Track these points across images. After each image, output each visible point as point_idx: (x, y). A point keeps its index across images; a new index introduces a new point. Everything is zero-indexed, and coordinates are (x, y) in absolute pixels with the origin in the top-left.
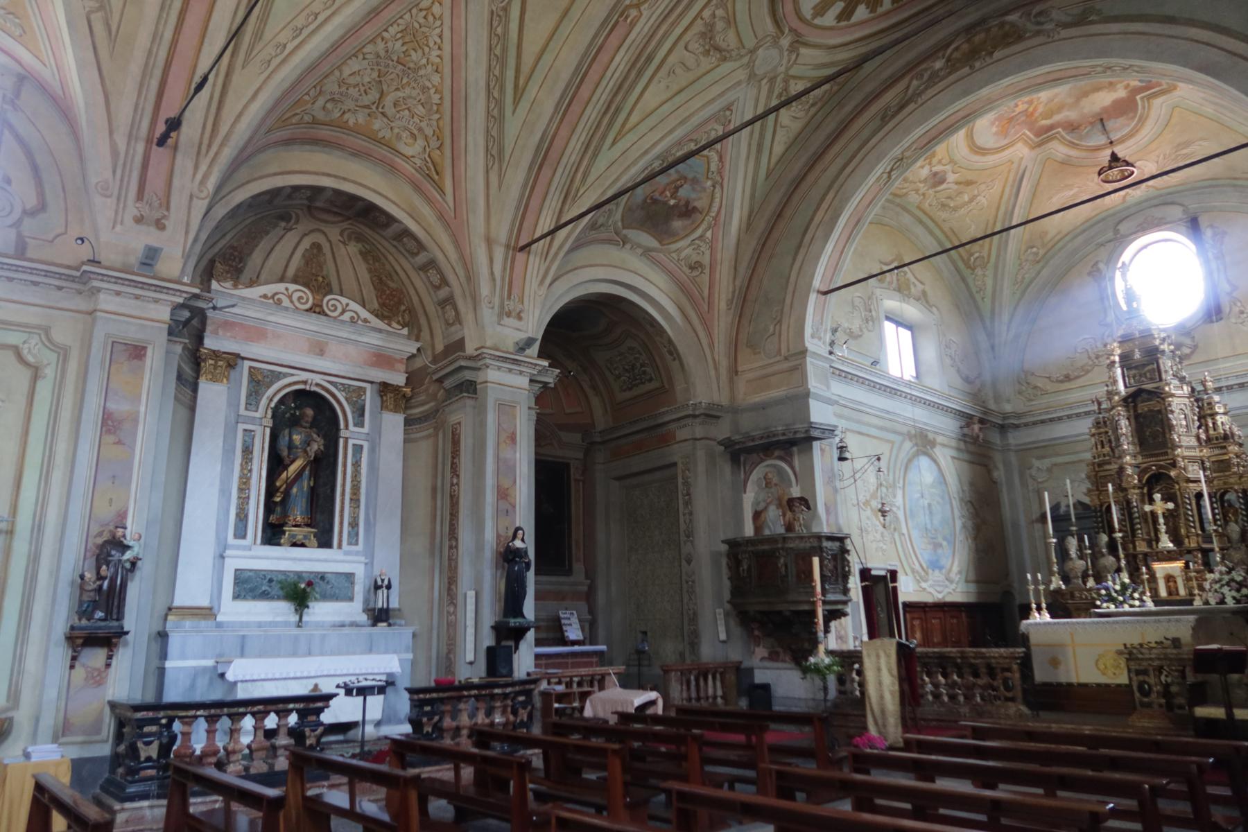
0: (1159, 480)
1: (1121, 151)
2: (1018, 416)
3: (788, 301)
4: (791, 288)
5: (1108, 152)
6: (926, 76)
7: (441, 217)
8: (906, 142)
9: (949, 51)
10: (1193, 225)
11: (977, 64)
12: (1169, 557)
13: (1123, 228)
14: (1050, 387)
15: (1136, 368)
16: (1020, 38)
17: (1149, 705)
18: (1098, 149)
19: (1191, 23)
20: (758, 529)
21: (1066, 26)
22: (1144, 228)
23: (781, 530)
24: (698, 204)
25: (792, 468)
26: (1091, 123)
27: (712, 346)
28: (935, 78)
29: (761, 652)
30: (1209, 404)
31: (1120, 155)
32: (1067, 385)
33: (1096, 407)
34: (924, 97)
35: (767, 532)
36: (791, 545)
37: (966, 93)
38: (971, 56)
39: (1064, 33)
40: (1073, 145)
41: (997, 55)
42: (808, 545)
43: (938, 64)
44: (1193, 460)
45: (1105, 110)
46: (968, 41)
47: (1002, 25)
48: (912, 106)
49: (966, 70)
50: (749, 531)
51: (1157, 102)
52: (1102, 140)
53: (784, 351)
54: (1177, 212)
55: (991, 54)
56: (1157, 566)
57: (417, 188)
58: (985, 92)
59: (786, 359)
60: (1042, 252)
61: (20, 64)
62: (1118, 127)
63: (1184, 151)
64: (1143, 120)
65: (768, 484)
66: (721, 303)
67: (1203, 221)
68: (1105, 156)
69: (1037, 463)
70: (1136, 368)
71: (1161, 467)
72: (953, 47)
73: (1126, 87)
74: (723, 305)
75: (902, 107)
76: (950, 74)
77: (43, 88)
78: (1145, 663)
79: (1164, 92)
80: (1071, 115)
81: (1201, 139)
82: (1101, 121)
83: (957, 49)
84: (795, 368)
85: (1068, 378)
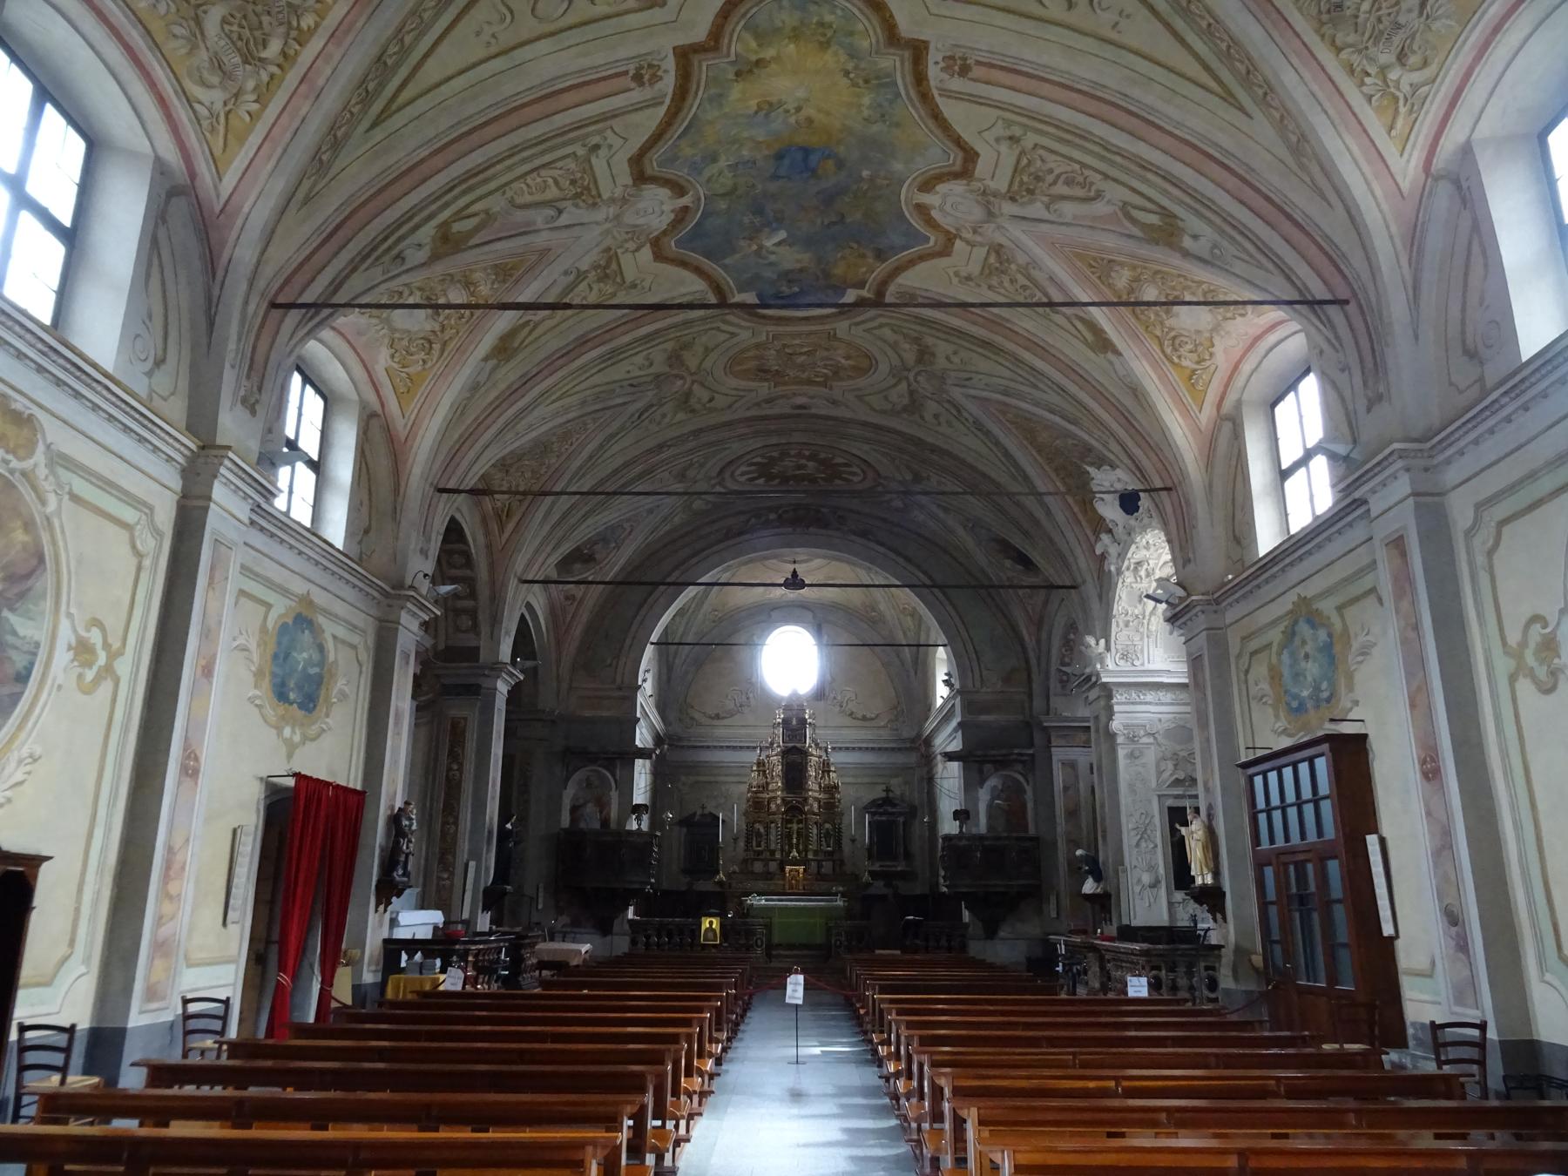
0: (794, 810)
2: (680, 739)
3: (628, 642)
5: (791, 567)
7: (489, 546)
10: (818, 629)
12: (795, 862)
13: (774, 614)
14: (704, 720)
16: (826, 526)
20: (574, 820)
21: (854, 533)
23: (597, 825)
24: (597, 556)
25: (614, 776)
27: (558, 661)
29: (564, 919)
32: (716, 722)
35: (582, 825)
41: (811, 529)
43: (772, 516)
44: (816, 799)
50: (565, 821)
53: (619, 680)
54: (809, 615)
56: (788, 868)
57: (484, 521)
59: (620, 689)
61: (383, 405)
65: (589, 785)
66: (577, 631)
69: (683, 778)
74: (578, 632)
75: (740, 534)
77: (388, 430)
84: (624, 698)
85: (718, 717)
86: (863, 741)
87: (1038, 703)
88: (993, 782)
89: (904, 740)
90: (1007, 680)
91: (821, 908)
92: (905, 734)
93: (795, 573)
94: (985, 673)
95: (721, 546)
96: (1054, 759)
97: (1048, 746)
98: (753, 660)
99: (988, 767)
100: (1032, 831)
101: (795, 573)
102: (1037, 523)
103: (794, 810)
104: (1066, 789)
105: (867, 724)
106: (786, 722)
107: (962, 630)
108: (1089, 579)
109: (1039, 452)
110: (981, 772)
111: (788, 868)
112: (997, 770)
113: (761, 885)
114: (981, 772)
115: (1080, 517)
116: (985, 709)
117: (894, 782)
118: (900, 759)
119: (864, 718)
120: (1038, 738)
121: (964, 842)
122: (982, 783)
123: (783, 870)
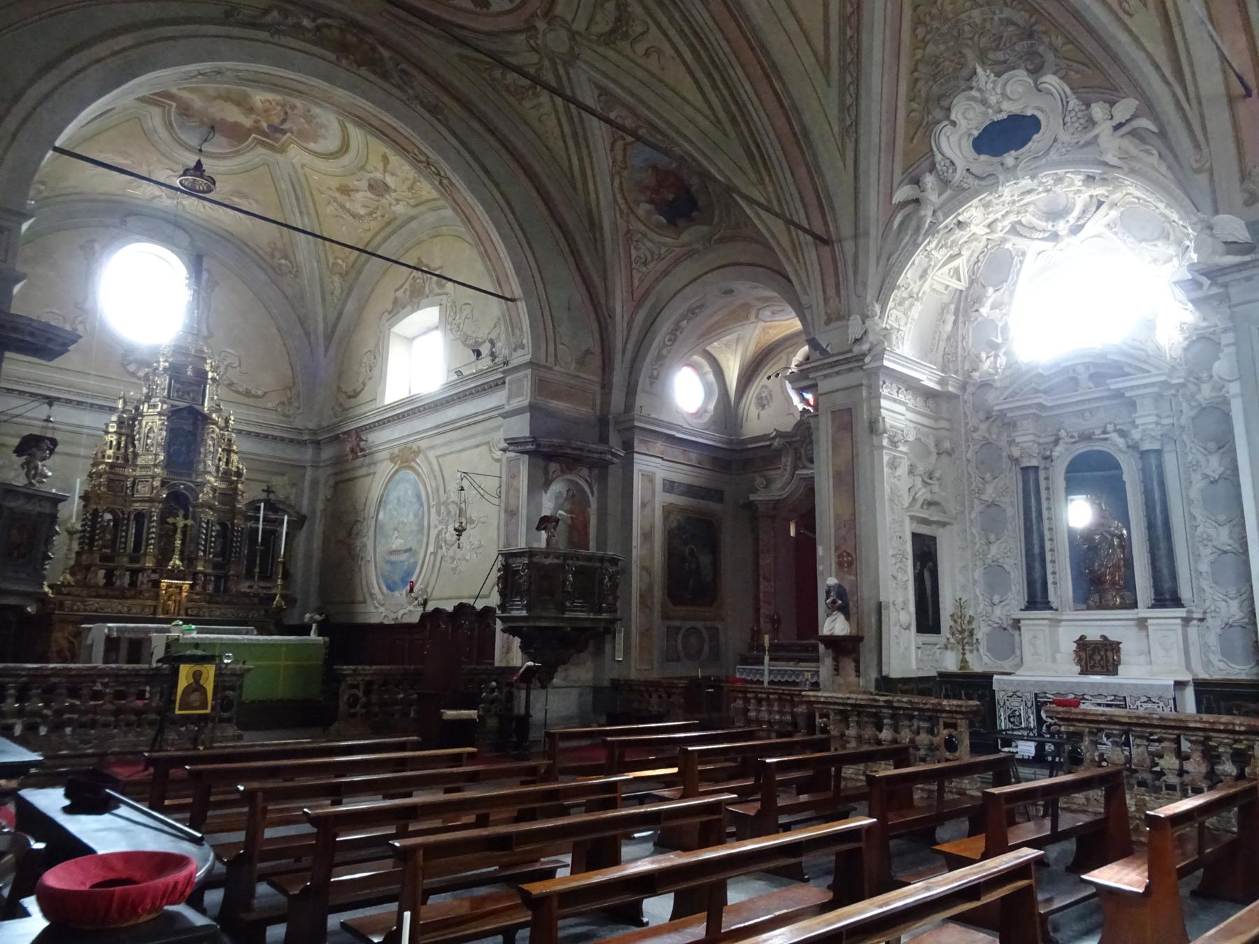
1: (208, 165)
4: (19, 111)
5: (197, 158)
6: (290, 21)
8: (242, 66)
9: (320, 21)
10: (197, 263)
11: (344, 62)
13: (131, 221)
15: (182, 383)
16: (385, 76)
17: (353, 716)
18: (189, 148)
19: (497, 185)
21: (422, 104)
22: (167, 240)
26: (202, 123)
28: (297, 31)
30: (230, 440)
31: (204, 167)
33: (120, 405)
34: (284, 40)
36: (12, 504)
37: (326, 78)
38: (342, 48)
39: (419, 108)
40: (169, 126)
42: (39, 509)
45: (223, 121)
46: (341, 30)
47: (373, 49)
48: (264, 35)
49: (333, 57)
51: (261, 150)
52: (194, 141)
54: (185, 240)
55: (359, 66)
56: (165, 582)
58: (341, 94)
60: (46, 194)
62: (219, 144)
63: (235, 199)
64: (237, 153)
67: (206, 263)
68: (191, 160)
70: (182, 383)
71: (187, 488)
72: (328, 21)
73: (257, 121)
76: (314, 43)
78: (360, 678)
79: (271, 148)
80: (197, 102)
81: (257, 201)
82: (213, 128)
83: (329, 26)
86: (249, 423)
87: (617, 399)
88: (558, 487)
89: (300, 431)
90: (581, 362)
91: (288, 645)
92: (298, 424)
93: (199, 164)
94: (560, 347)
95: (212, 29)
96: (636, 468)
97: (628, 447)
98: (87, 276)
99: (553, 466)
100: (592, 548)
101: (199, 164)
102: (800, 139)
103: (178, 501)
104: (644, 505)
105: (251, 401)
106: (175, 371)
107: (540, 285)
108: (873, 232)
109: (917, 22)
110: (546, 472)
111: (165, 582)
112: (563, 472)
113: (116, 606)
114: (546, 472)
115: (900, 143)
116: (556, 395)
117: (279, 482)
118: (290, 453)
119: (248, 394)
120: (614, 440)
121: (547, 561)
122: (547, 484)
123: (156, 584)
